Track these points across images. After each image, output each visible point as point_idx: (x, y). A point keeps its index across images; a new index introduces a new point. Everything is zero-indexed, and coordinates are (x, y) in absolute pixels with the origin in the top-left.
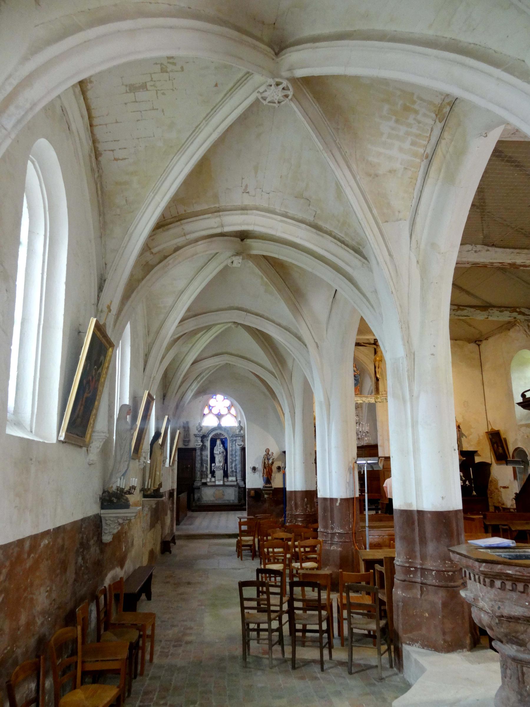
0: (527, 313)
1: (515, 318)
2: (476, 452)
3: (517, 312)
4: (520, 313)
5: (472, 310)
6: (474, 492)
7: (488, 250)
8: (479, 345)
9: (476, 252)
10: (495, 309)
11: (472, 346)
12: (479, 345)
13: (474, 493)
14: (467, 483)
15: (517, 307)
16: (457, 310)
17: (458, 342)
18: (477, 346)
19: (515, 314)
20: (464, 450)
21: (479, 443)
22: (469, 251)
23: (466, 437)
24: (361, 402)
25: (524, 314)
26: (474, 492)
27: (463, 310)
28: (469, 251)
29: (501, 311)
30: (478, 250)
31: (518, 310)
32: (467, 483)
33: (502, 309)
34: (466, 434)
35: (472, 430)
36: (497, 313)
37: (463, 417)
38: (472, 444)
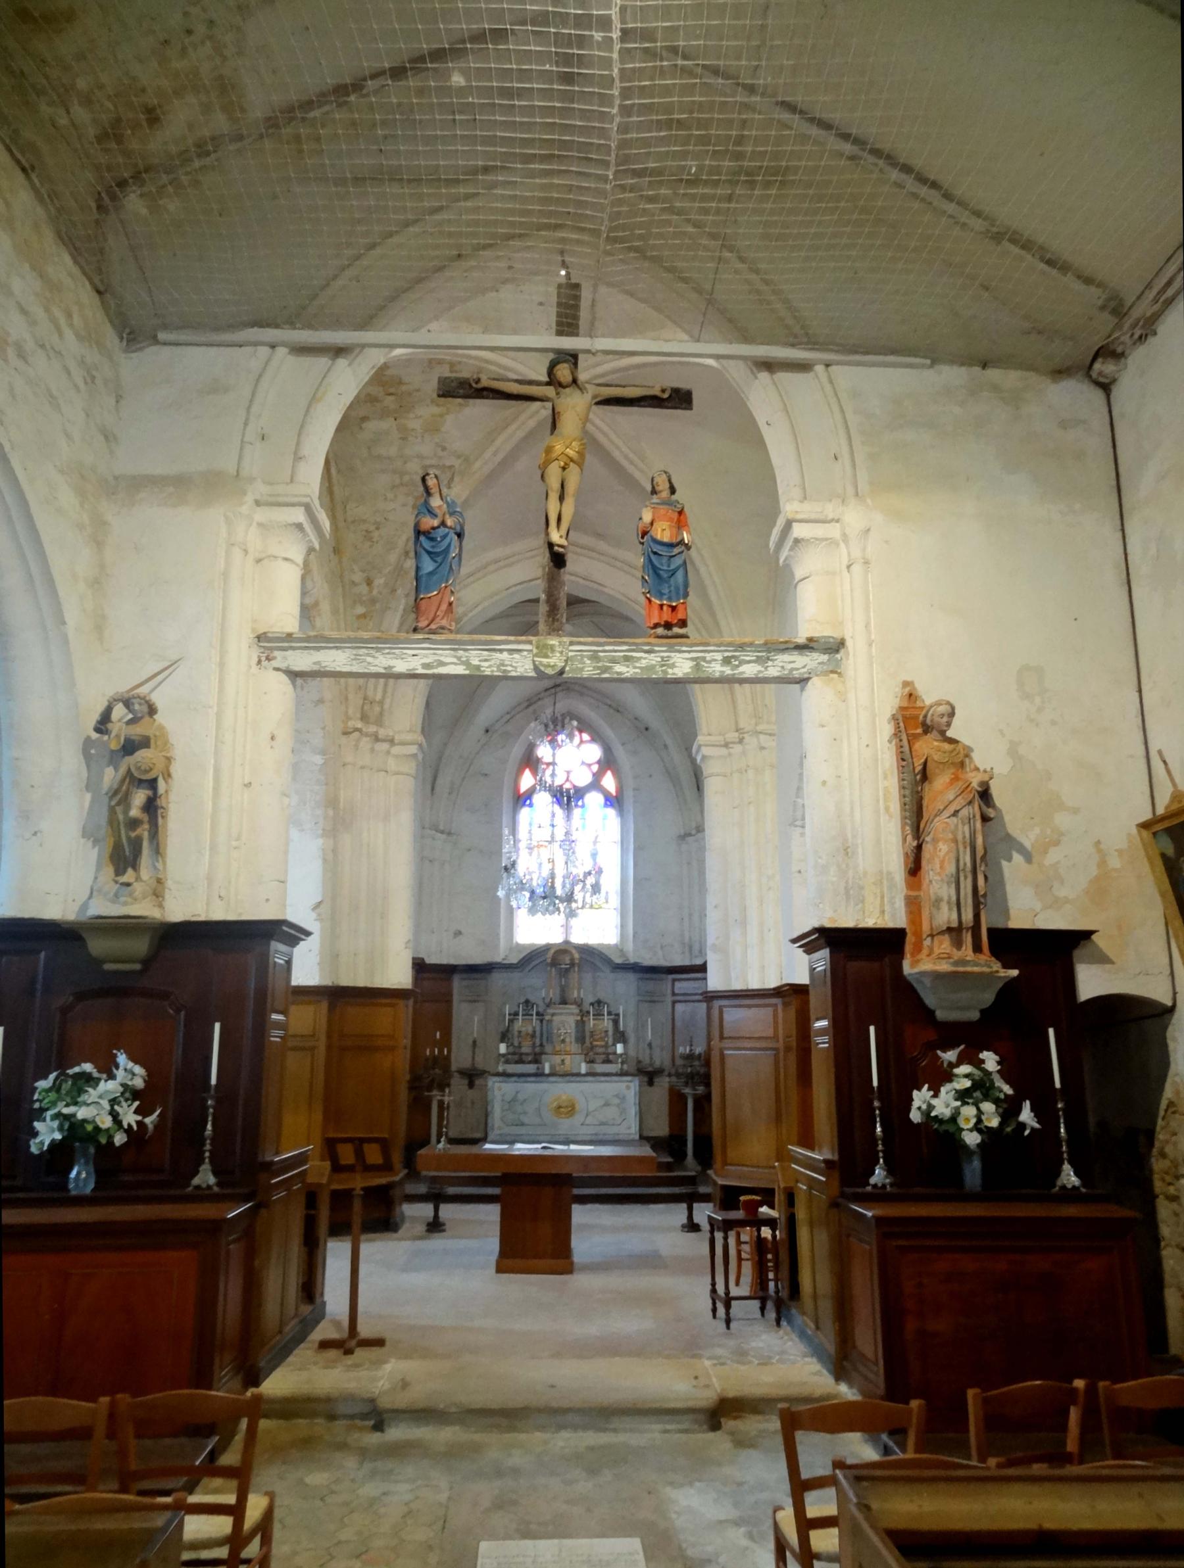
2: (1086, 935)
6: (1067, 1168)
8: (1106, 387)
11: (1075, 395)
12: (1106, 387)
13: (1069, 1177)
14: (1026, 1115)
17: (993, 374)
18: (1098, 395)
20: (1015, 923)
21: (1100, 889)
23: (1028, 857)
24: (460, 670)
26: (1067, 1168)
32: (1026, 1115)
34: (1028, 844)
35: (1062, 820)
37: (1013, 751)
38: (1062, 892)
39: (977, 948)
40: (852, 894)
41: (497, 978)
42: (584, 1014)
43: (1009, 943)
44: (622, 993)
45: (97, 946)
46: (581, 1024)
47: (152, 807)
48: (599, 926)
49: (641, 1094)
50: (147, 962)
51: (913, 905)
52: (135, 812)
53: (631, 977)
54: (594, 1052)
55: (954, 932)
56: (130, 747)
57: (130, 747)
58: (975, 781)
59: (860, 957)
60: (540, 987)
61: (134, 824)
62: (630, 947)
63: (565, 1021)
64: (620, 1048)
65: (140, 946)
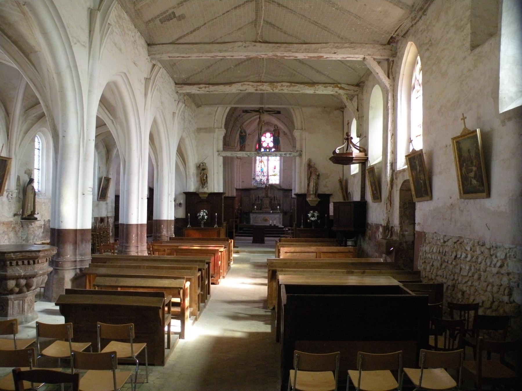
0: (346, 88)
1: (337, 92)
3: (338, 87)
4: (341, 88)
5: (302, 86)
7: (255, 46)
8: (343, 112)
9: (245, 47)
10: (320, 86)
15: (339, 83)
16: (290, 86)
18: (341, 113)
19: (337, 89)
22: (239, 47)
25: (343, 89)
27: (295, 86)
28: (239, 47)
29: (325, 87)
30: (247, 45)
31: (339, 86)
33: (326, 85)
36: (323, 88)
39: (315, 197)
40: (301, 188)
41: (252, 192)
42: (271, 199)
43: (320, 196)
44: (279, 195)
45: (201, 196)
46: (270, 202)
47: (206, 177)
48: (275, 180)
49: (283, 218)
50: (207, 197)
51: (308, 190)
52: (205, 178)
53: (281, 191)
54: (273, 208)
55: (313, 194)
56: (203, 169)
57: (203, 169)
58: (318, 174)
59: (301, 197)
60: (262, 194)
61: (204, 180)
62: (281, 185)
63: (267, 202)
64: (278, 207)
65: (207, 195)
